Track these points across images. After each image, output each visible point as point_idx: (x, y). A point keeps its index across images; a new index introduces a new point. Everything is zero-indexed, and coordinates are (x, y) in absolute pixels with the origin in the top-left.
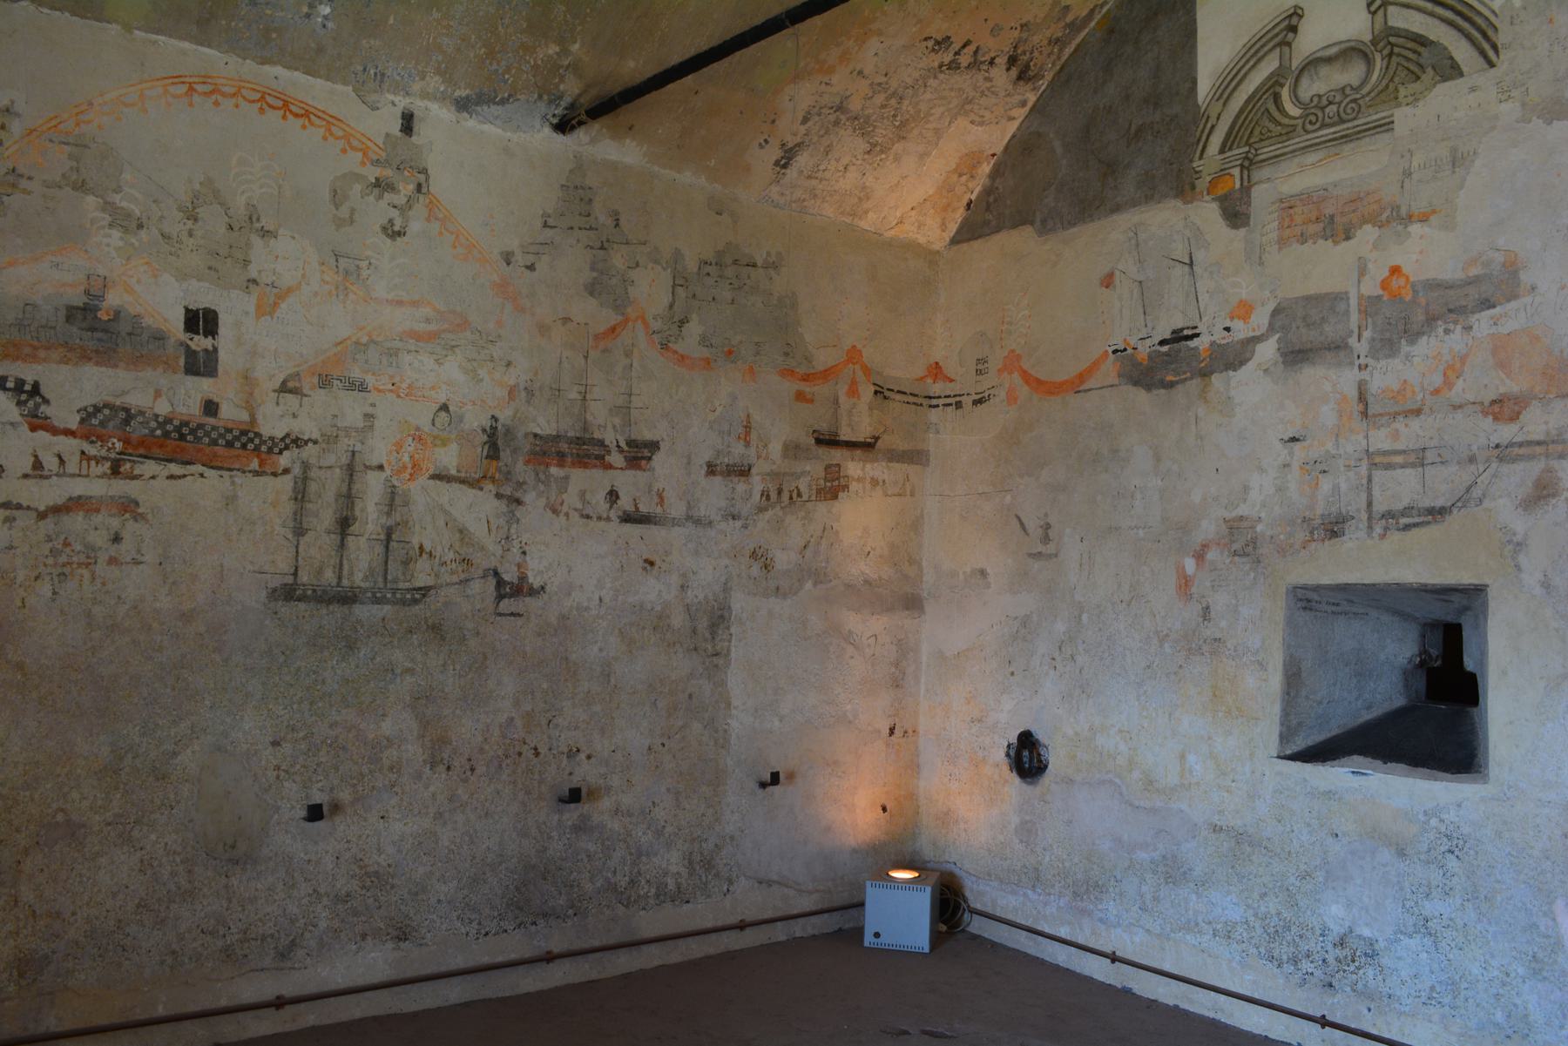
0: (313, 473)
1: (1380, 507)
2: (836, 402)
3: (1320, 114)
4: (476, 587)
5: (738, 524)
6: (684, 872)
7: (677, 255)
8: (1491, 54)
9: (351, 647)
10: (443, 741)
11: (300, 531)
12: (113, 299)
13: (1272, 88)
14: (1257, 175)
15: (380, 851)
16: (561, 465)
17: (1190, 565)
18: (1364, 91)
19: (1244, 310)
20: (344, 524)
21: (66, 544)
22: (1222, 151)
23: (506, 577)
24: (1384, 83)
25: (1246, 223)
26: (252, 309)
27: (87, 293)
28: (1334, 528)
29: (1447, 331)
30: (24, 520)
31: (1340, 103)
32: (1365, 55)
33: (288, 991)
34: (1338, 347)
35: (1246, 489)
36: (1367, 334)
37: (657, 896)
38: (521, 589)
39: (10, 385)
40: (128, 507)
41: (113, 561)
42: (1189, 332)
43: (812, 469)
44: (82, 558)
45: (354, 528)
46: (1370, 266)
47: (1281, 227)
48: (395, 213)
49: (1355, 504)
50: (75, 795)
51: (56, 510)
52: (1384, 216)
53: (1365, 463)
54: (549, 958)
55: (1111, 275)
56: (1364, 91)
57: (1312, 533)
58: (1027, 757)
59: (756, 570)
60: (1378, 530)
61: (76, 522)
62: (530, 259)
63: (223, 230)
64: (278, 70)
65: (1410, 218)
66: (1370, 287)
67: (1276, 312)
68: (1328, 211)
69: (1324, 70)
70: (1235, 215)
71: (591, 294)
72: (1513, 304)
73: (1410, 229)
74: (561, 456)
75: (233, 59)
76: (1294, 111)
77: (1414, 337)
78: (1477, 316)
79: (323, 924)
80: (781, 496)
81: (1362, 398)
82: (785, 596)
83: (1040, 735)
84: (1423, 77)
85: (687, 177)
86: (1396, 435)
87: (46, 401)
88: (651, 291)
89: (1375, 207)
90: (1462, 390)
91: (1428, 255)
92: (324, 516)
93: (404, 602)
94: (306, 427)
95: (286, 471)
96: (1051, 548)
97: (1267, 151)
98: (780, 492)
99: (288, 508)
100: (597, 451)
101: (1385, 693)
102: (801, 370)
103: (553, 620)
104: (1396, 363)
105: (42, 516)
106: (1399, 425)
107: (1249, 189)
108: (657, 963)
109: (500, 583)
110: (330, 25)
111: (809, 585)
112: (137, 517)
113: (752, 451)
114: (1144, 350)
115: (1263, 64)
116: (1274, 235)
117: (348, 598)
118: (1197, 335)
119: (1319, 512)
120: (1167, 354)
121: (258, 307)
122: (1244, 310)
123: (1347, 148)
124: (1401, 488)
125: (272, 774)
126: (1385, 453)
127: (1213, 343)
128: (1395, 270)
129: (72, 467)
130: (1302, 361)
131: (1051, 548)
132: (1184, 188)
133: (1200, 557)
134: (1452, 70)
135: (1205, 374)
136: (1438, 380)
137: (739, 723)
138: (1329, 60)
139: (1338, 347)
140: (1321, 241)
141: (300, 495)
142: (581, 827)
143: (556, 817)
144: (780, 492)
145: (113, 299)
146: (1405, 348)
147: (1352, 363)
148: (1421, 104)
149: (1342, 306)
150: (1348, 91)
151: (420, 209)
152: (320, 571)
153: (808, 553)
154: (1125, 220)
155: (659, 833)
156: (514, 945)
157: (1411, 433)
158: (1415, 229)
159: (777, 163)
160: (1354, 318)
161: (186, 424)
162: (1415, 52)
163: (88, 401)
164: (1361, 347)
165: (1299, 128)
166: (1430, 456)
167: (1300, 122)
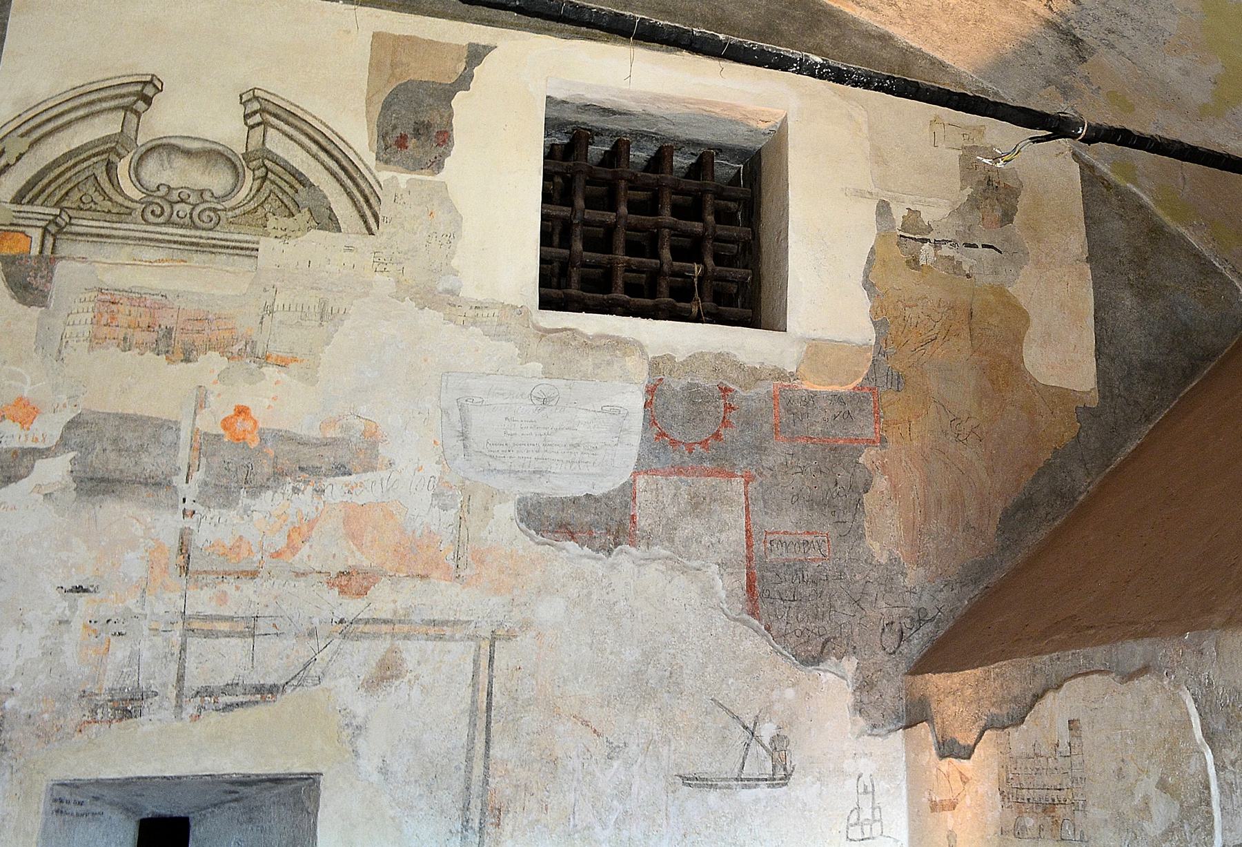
1: (194, 681)
8: (371, 221)
14: (65, 248)
18: (228, 204)
24: (252, 205)
28: (127, 706)
29: (296, 490)
31: (195, 206)
46: (211, 398)
47: (95, 322)
49: (161, 677)
52: (235, 349)
53: (179, 628)
56: (228, 204)
57: (94, 711)
60: (190, 709)
68: (166, 322)
73: (264, 370)
77: (257, 490)
78: (331, 480)
84: (298, 216)
89: (227, 334)
90: (305, 557)
91: (281, 403)
97: (85, 224)
104: (232, 515)
106: (229, 587)
107: (53, 260)
115: (97, 121)
119: (107, 684)
123: (198, 258)
124: (225, 660)
126: (206, 618)
136: (280, 542)
140: (149, 354)
146: (244, 499)
148: (292, 242)
150: (207, 196)
157: (242, 598)
160: (184, 456)
162: (292, 187)
164: (189, 490)
165: (138, 213)
166: (263, 626)
167: (140, 207)
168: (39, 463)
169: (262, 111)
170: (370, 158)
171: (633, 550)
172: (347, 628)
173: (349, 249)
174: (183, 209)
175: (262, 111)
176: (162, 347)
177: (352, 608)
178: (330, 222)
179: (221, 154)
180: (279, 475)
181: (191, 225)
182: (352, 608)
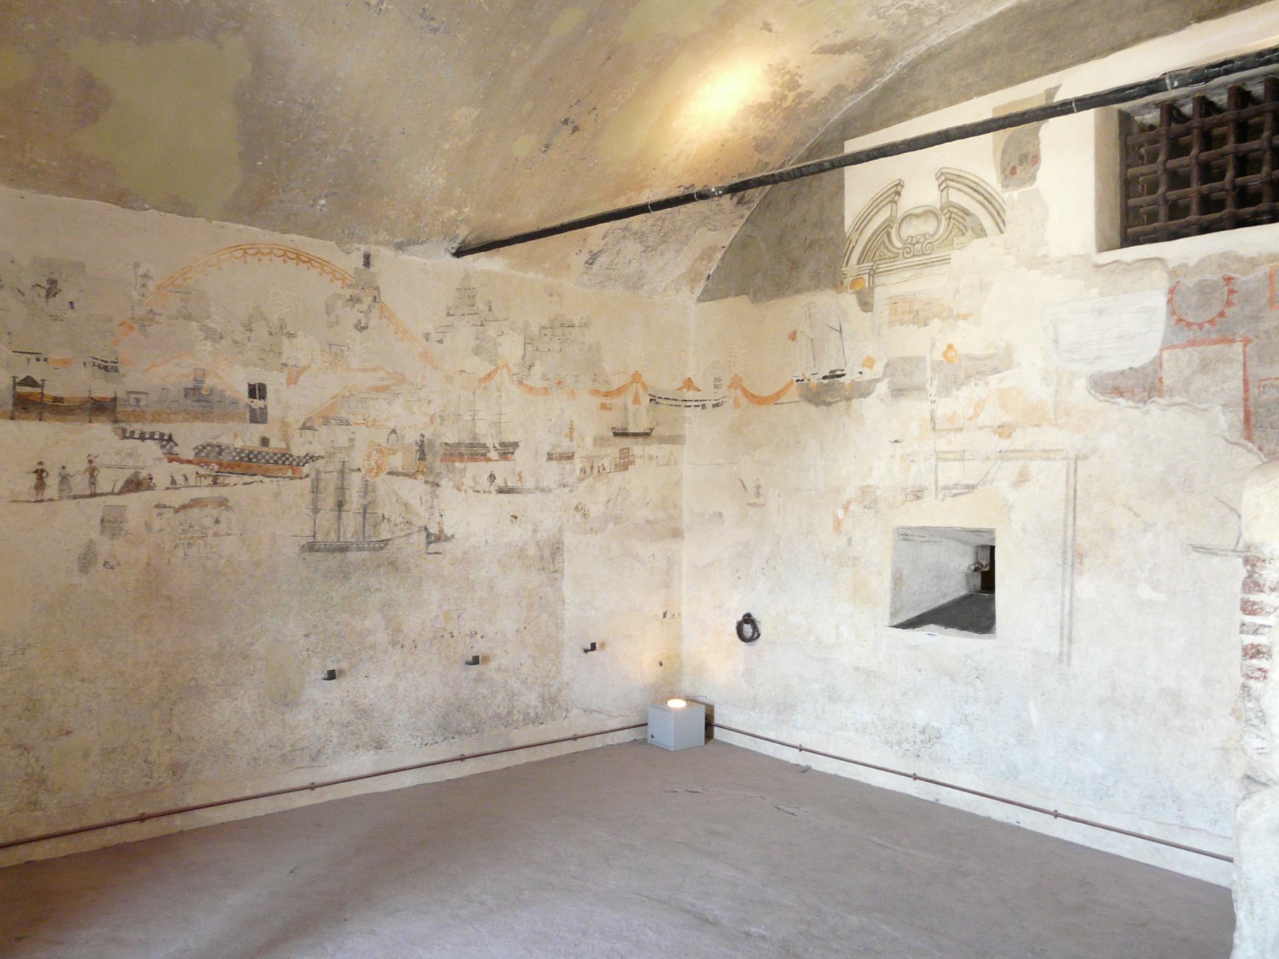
0: (322, 476)
2: (626, 409)
4: (415, 537)
5: (567, 490)
6: (540, 705)
7: (527, 324)
9: (347, 577)
10: (398, 630)
11: (316, 511)
12: (209, 382)
13: (886, 228)
15: (366, 696)
16: (461, 461)
17: (840, 513)
19: (870, 362)
20: (340, 505)
21: (191, 526)
23: (432, 531)
25: (871, 310)
26: (284, 381)
27: (195, 380)
30: (168, 514)
32: (936, 216)
33: (318, 780)
35: (871, 469)
36: (935, 382)
37: (524, 720)
38: (440, 538)
39: (157, 436)
40: (222, 503)
41: (215, 534)
43: (611, 453)
44: (198, 534)
45: (345, 507)
48: (361, 315)
50: (200, 670)
51: (184, 507)
54: (463, 758)
55: (795, 333)
58: (748, 629)
59: (578, 518)
61: (195, 513)
62: (439, 336)
63: (266, 336)
64: (294, 236)
65: (958, 317)
66: (937, 356)
67: (887, 365)
69: (915, 221)
70: (866, 304)
71: (476, 354)
72: (1008, 372)
74: (461, 455)
75: (268, 232)
76: (899, 245)
77: (959, 386)
79: (335, 740)
80: (592, 470)
81: (932, 419)
82: (596, 533)
83: (755, 616)
85: (531, 275)
86: (950, 442)
87: (176, 445)
88: (511, 348)
92: (329, 502)
93: (374, 549)
94: (317, 449)
95: (307, 476)
96: (761, 500)
98: (592, 468)
99: (309, 497)
100: (482, 451)
101: (955, 587)
102: (603, 390)
103: (459, 555)
105: (177, 511)
108: (524, 761)
109: (429, 535)
110: (325, 210)
111: (611, 525)
112: (229, 508)
113: (575, 443)
114: (815, 380)
117: (344, 549)
121: (288, 380)
122: (870, 362)
125: (305, 653)
128: (950, 347)
129: (192, 482)
131: (761, 500)
132: (837, 284)
133: (846, 508)
134: (981, 232)
135: (848, 399)
137: (570, 613)
138: (918, 216)
139: (919, 389)
141: (315, 490)
142: (479, 680)
143: (464, 674)
144: (592, 468)
145: (209, 382)
151: (375, 312)
152: (328, 534)
153: (610, 505)
154: (805, 298)
155: (524, 682)
156: (442, 751)
159: (587, 262)
161: (251, 452)
163: (199, 442)
164: (932, 390)
171: (1160, 400)
172: (1004, 455)
177: (1005, 444)
180: (968, 377)
182: (1005, 444)
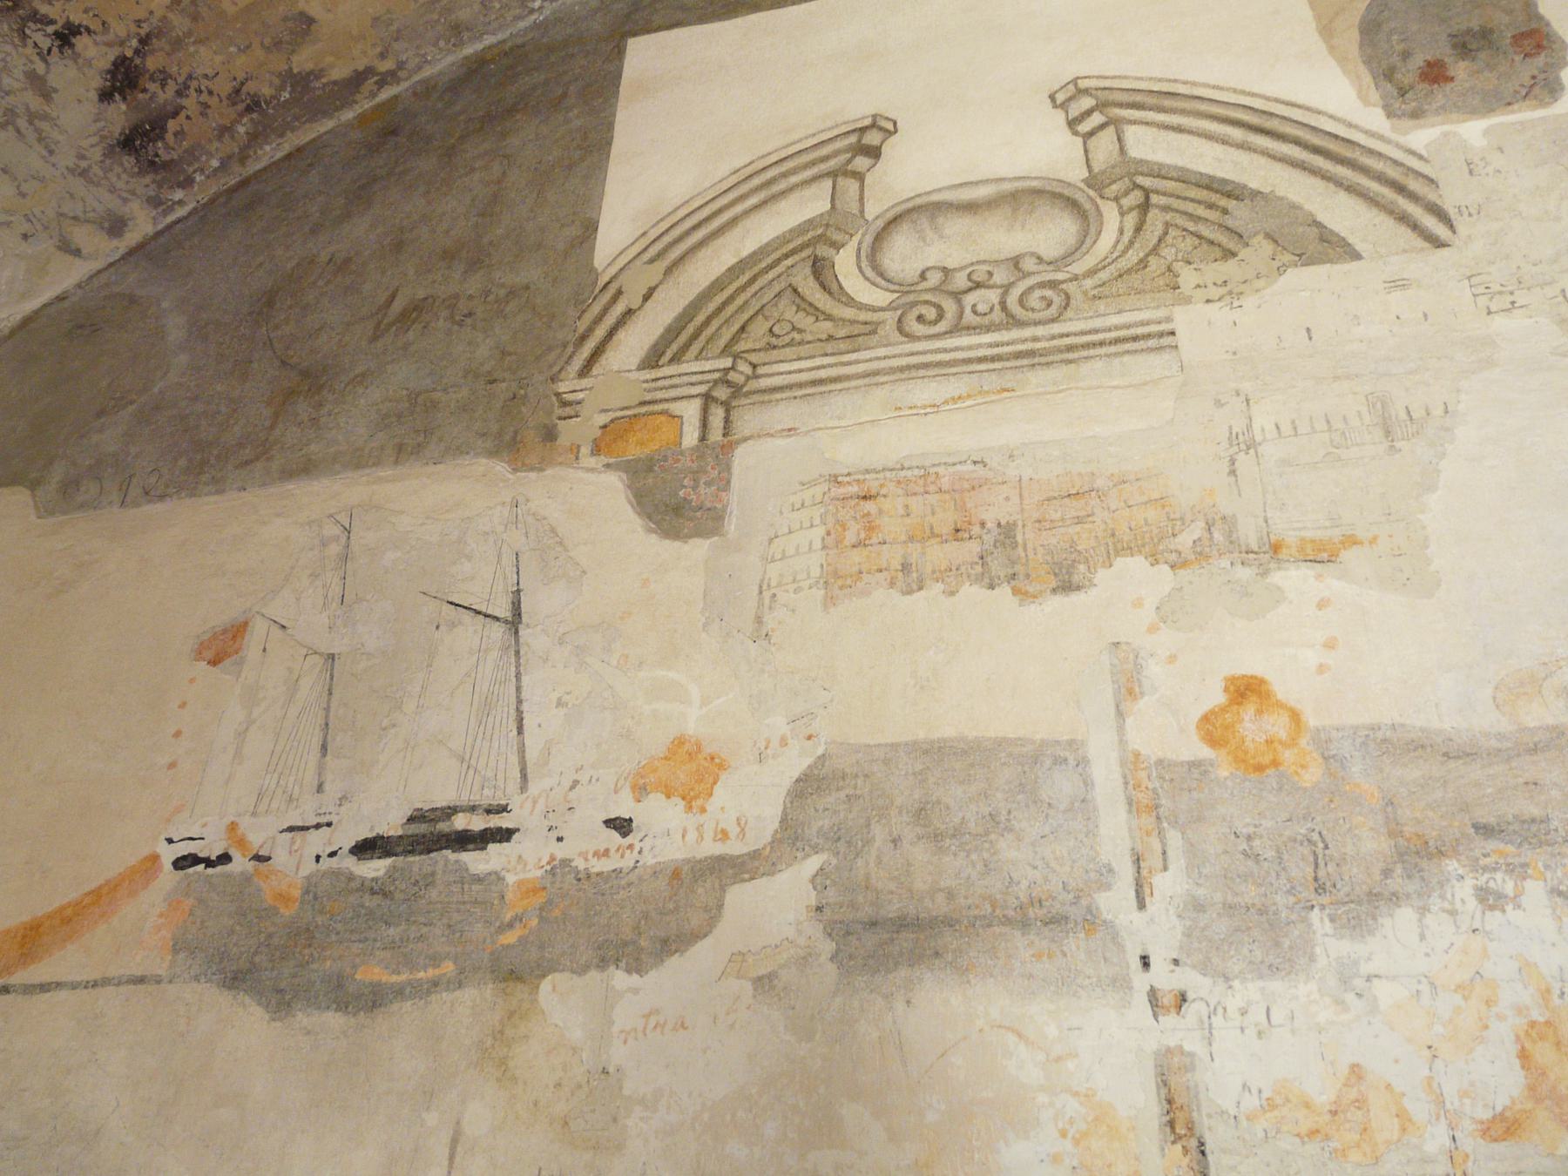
3: (949, 306)
8: (1430, 222)
18: (1078, 268)
19: (691, 770)
22: (652, 359)
24: (1133, 257)
31: (1007, 288)
34: (1056, 921)
36: (1169, 884)
42: (477, 823)
46: (1154, 670)
52: (1185, 540)
56: (1078, 268)
67: (807, 786)
73: (1277, 577)
84: (1244, 253)
97: (783, 369)
107: (728, 448)
114: (295, 864)
115: (783, 204)
116: (814, 563)
118: (505, 835)
120: (377, 889)
123: (1037, 379)
127: (559, 867)
128: (1246, 690)
130: (915, 958)
135: (516, 973)
139: (1057, 918)
140: (971, 592)
147: (1121, 983)
148: (1249, 302)
149: (1061, 786)
150: (1029, 264)
158: (1294, 579)
162: (1211, 206)
165: (889, 328)
167: (891, 318)
168: (740, 897)
169: (1101, 106)
170: (1375, 119)
173: (1398, 284)
174: (986, 299)
175: (1101, 106)
176: (997, 567)
178: (1331, 247)
179: (1038, 192)
181: (1008, 322)
